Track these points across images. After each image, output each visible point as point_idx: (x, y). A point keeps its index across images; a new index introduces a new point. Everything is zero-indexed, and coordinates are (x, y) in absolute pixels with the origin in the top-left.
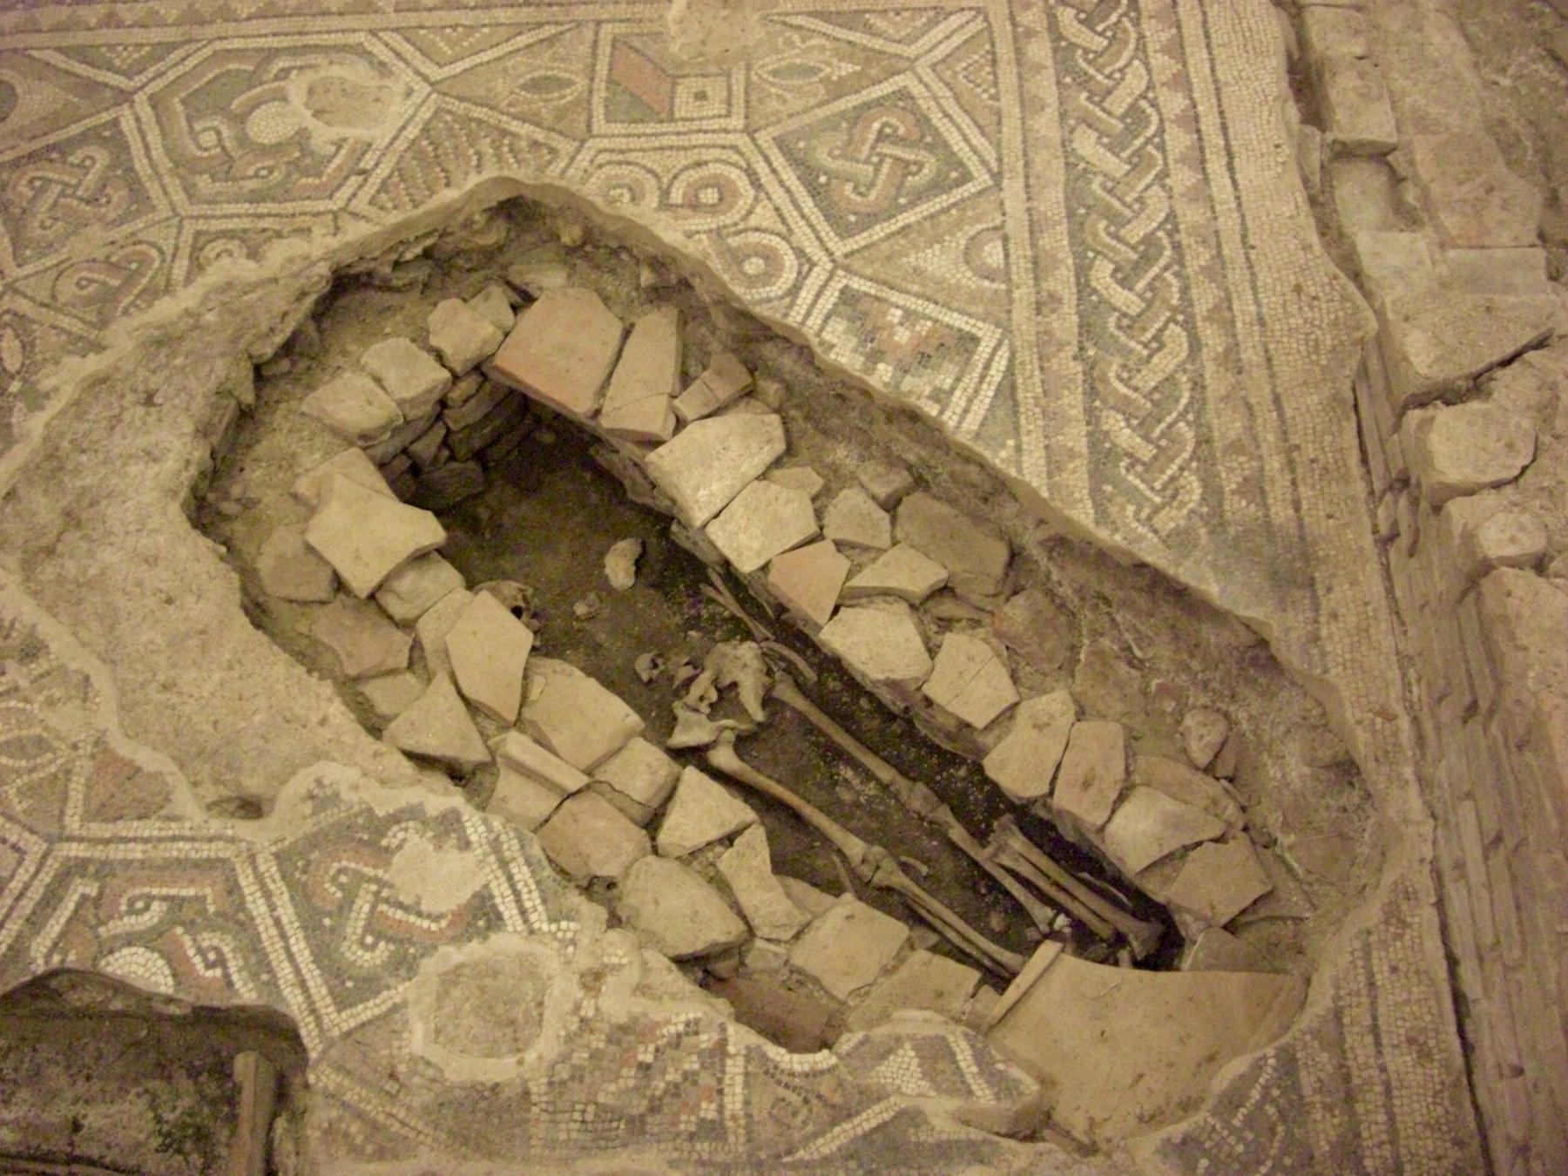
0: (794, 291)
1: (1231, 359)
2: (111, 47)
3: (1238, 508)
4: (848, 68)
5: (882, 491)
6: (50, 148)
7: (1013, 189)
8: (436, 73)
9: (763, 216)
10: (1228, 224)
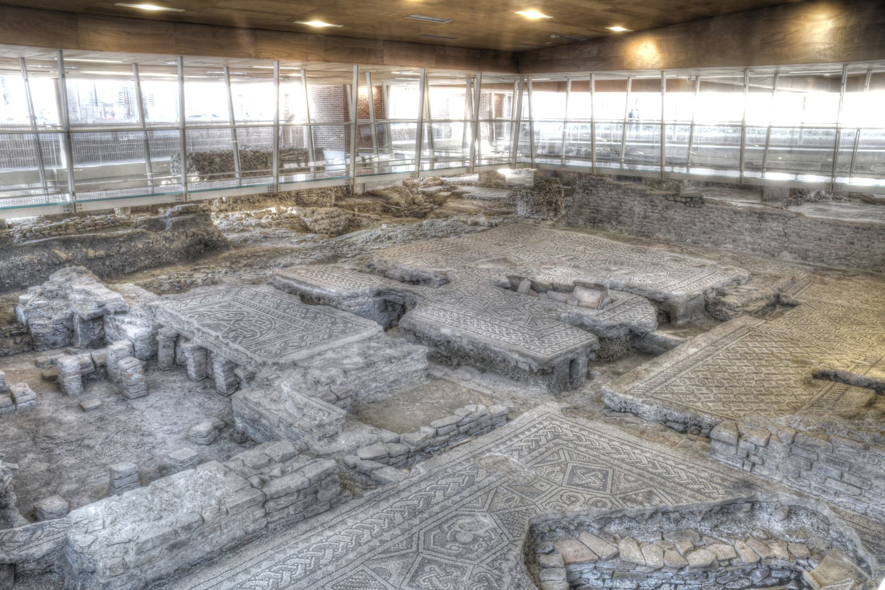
0: (613, 503)
1: (688, 467)
2: (394, 546)
3: (726, 483)
4: (558, 468)
5: (660, 538)
6: (416, 572)
7: (616, 468)
8: (485, 509)
9: (587, 497)
10: (654, 452)
